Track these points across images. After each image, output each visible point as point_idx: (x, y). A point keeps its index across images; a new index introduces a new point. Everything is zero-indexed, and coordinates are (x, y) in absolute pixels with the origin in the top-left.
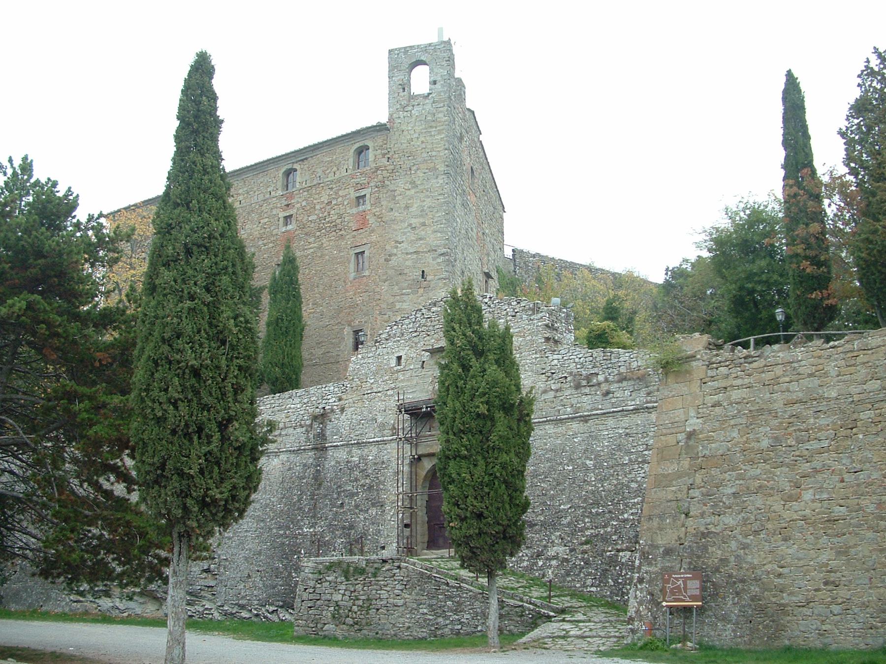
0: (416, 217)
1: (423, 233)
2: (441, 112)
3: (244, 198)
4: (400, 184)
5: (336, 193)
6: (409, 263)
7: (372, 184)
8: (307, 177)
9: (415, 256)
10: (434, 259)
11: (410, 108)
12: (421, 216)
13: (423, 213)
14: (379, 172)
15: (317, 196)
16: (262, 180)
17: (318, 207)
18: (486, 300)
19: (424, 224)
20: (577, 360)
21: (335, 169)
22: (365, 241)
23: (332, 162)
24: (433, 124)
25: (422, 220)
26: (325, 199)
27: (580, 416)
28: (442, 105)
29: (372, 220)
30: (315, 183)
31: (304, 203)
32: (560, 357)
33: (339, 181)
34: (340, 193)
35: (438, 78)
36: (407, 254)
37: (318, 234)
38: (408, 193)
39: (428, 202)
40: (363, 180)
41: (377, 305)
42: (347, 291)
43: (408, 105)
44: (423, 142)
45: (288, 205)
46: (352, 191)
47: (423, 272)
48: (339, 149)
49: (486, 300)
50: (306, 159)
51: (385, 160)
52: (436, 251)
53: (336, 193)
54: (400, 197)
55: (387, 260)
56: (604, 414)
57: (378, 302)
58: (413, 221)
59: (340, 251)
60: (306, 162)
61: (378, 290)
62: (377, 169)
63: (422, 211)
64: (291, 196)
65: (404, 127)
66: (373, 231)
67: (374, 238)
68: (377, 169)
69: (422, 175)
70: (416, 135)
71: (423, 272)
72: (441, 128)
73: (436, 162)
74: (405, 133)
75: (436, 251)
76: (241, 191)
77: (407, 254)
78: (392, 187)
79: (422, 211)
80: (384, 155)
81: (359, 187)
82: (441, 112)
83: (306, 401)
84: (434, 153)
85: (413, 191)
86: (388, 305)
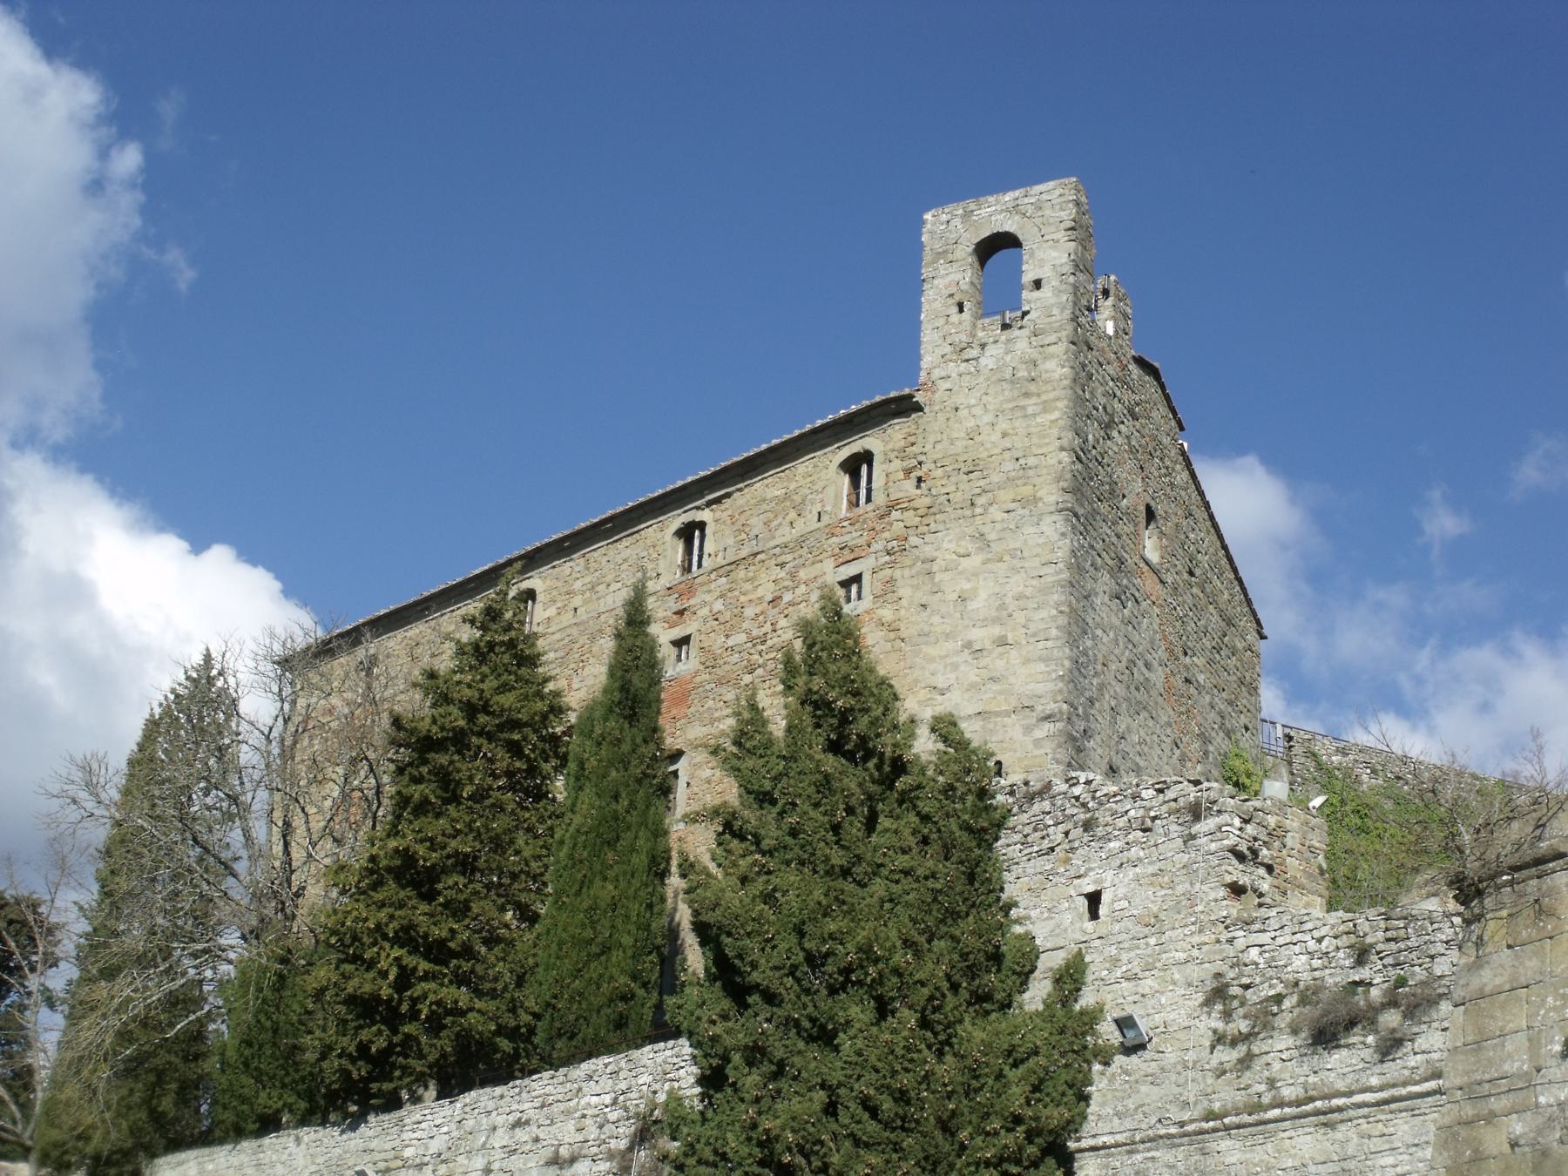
0: (985, 622)
1: (1000, 664)
2: (1052, 356)
3: (586, 602)
4: (947, 543)
5: (793, 576)
7: (876, 546)
8: (731, 541)
10: (1028, 730)
11: (974, 353)
12: (997, 620)
13: (1002, 614)
14: (895, 515)
15: (748, 586)
16: (623, 555)
17: (750, 612)
18: (1077, 791)
19: (1002, 642)
20: (1312, 945)
21: (793, 515)
23: (787, 497)
24: (1032, 388)
25: (997, 631)
26: (767, 591)
27: (1317, 1113)
28: (1053, 338)
30: (744, 553)
31: (718, 606)
32: (1264, 938)
33: (800, 542)
34: (802, 574)
35: (1045, 273)
37: (747, 679)
38: (966, 563)
39: (1017, 584)
40: (853, 537)
43: (969, 345)
44: (1004, 435)
45: (680, 613)
46: (829, 564)
48: (803, 467)
49: (1077, 791)
50: (728, 495)
51: (909, 485)
52: (1031, 708)
53: (793, 576)
54: (947, 576)
56: (1386, 1102)
58: (980, 635)
60: (727, 502)
62: (891, 507)
63: (1003, 606)
64: (690, 591)
65: (959, 399)
68: (891, 507)
69: (999, 516)
70: (988, 418)
72: (1051, 395)
73: (1037, 481)
74: (963, 413)
75: (1031, 708)
76: (578, 585)
78: (928, 551)
79: (1003, 606)
80: (908, 472)
81: (849, 554)
82: (1052, 356)
83: (623, 1086)
84: (1032, 461)
85: (975, 561)
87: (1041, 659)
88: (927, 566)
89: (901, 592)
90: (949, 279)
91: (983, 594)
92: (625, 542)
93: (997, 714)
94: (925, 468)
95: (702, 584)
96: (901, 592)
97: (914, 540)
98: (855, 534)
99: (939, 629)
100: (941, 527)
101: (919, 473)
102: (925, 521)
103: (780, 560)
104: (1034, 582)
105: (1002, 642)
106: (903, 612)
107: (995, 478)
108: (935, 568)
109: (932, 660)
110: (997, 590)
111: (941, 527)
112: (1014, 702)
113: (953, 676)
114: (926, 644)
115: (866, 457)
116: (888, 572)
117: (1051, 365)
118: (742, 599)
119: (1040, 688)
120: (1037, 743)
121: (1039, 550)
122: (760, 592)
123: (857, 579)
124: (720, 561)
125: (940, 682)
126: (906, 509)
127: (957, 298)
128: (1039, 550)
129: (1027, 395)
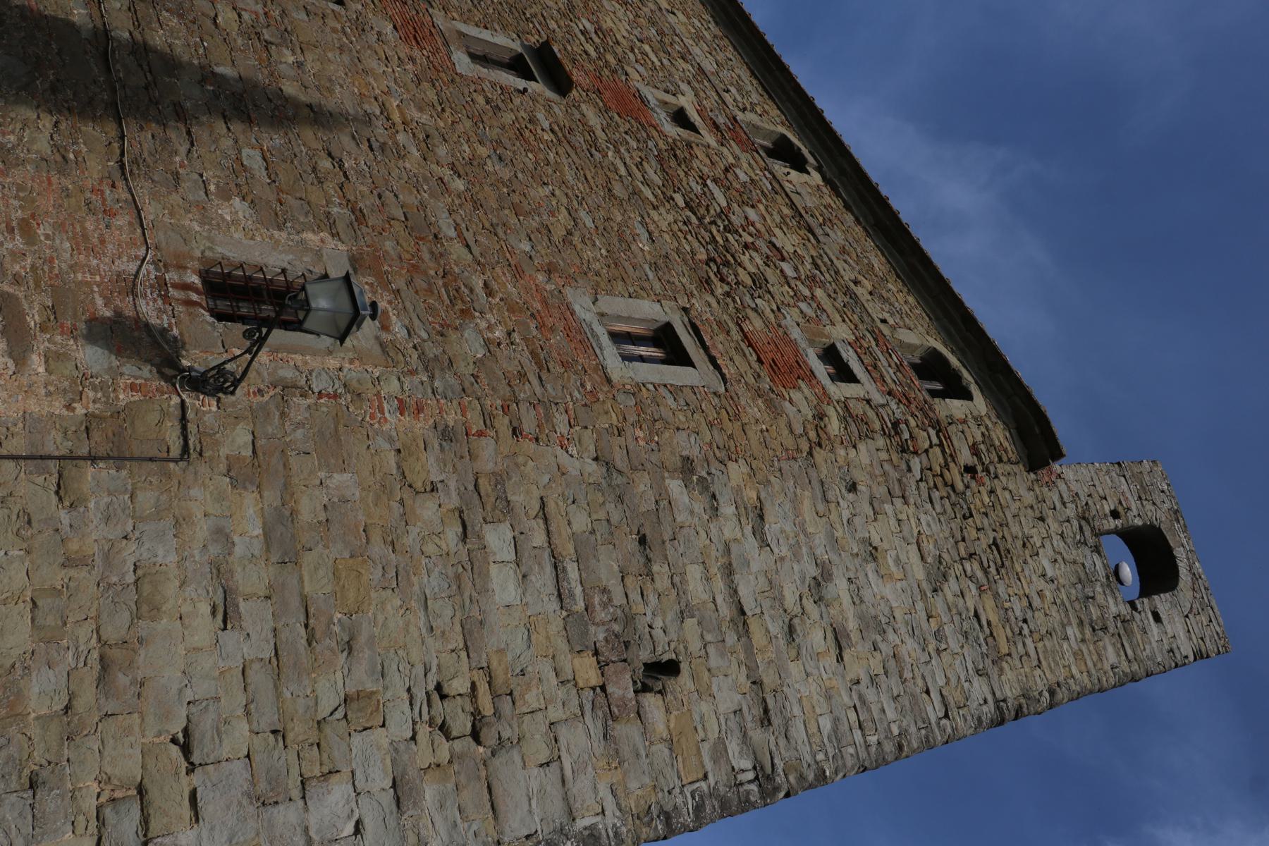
0: (857, 600)
6: (694, 573)
9: (726, 611)
13: (875, 626)
15: (778, 219)
22: (729, 371)
25: (852, 625)
29: (799, 403)
36: (729, 571)
39: (910, 648)
41: (488, 418)
42: (517, 272)
47: (671, 668)
52: (765, 719)
55: (687, 467)
57: (503, 423)
58: (839, 587)
59: (655, 266)
61: (561, 421)
62: (937, 425)
66: (773, 409)
67: (754, 410)
68: (937, 425)
71: (671, 668)
75: (765, 719)
77: (729, 571)
85: (919, 572)
86: (499, 479)
87: (836, 721)
88: (897, 492)
89: (862, 447)
90: (1128, 495)
91: (888, 590)
92: (755, 82)
93: (749, 649)
94: (986, 480)
95: (753, 157)
96: (862, 447)
97: (916, 464)
98: (891, 371)
99: (834, 517)
100: (939, 509)
101: (979, 468)
102: (939, 481)
103: (819, 262)
104: (920, 682)
105: (839, 640)
106: (842, 452)
107: (1001, 588)
108: (898, 502)
109: (797, 512)
110: (898, 614)
111: (939, 509)
112: (769, 679)
113: (785, 551)
114: (814, 498)
115: (957, 390)
116: (877, 426)
117: (1111, 656)
118: (761, 207)
119: (798, 732)
120: (720, 751)
121: (953, 681)
122: (777, 231)
123: (850, 377)
124: (787, 186)
125: (773, 527)
126: (943, 452)
127: (1120, 509)
128: (953, 681)
129: (1081, 623)
